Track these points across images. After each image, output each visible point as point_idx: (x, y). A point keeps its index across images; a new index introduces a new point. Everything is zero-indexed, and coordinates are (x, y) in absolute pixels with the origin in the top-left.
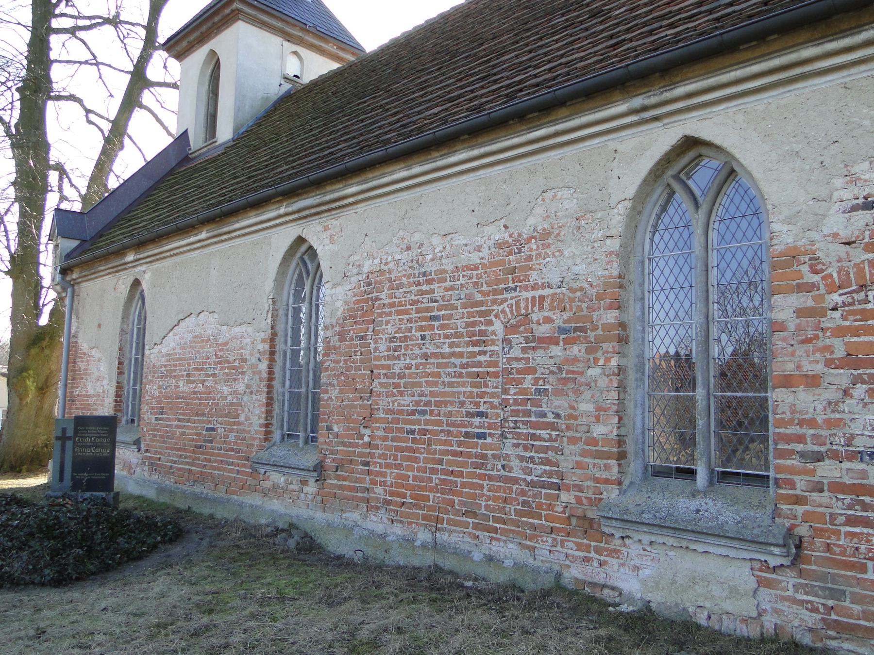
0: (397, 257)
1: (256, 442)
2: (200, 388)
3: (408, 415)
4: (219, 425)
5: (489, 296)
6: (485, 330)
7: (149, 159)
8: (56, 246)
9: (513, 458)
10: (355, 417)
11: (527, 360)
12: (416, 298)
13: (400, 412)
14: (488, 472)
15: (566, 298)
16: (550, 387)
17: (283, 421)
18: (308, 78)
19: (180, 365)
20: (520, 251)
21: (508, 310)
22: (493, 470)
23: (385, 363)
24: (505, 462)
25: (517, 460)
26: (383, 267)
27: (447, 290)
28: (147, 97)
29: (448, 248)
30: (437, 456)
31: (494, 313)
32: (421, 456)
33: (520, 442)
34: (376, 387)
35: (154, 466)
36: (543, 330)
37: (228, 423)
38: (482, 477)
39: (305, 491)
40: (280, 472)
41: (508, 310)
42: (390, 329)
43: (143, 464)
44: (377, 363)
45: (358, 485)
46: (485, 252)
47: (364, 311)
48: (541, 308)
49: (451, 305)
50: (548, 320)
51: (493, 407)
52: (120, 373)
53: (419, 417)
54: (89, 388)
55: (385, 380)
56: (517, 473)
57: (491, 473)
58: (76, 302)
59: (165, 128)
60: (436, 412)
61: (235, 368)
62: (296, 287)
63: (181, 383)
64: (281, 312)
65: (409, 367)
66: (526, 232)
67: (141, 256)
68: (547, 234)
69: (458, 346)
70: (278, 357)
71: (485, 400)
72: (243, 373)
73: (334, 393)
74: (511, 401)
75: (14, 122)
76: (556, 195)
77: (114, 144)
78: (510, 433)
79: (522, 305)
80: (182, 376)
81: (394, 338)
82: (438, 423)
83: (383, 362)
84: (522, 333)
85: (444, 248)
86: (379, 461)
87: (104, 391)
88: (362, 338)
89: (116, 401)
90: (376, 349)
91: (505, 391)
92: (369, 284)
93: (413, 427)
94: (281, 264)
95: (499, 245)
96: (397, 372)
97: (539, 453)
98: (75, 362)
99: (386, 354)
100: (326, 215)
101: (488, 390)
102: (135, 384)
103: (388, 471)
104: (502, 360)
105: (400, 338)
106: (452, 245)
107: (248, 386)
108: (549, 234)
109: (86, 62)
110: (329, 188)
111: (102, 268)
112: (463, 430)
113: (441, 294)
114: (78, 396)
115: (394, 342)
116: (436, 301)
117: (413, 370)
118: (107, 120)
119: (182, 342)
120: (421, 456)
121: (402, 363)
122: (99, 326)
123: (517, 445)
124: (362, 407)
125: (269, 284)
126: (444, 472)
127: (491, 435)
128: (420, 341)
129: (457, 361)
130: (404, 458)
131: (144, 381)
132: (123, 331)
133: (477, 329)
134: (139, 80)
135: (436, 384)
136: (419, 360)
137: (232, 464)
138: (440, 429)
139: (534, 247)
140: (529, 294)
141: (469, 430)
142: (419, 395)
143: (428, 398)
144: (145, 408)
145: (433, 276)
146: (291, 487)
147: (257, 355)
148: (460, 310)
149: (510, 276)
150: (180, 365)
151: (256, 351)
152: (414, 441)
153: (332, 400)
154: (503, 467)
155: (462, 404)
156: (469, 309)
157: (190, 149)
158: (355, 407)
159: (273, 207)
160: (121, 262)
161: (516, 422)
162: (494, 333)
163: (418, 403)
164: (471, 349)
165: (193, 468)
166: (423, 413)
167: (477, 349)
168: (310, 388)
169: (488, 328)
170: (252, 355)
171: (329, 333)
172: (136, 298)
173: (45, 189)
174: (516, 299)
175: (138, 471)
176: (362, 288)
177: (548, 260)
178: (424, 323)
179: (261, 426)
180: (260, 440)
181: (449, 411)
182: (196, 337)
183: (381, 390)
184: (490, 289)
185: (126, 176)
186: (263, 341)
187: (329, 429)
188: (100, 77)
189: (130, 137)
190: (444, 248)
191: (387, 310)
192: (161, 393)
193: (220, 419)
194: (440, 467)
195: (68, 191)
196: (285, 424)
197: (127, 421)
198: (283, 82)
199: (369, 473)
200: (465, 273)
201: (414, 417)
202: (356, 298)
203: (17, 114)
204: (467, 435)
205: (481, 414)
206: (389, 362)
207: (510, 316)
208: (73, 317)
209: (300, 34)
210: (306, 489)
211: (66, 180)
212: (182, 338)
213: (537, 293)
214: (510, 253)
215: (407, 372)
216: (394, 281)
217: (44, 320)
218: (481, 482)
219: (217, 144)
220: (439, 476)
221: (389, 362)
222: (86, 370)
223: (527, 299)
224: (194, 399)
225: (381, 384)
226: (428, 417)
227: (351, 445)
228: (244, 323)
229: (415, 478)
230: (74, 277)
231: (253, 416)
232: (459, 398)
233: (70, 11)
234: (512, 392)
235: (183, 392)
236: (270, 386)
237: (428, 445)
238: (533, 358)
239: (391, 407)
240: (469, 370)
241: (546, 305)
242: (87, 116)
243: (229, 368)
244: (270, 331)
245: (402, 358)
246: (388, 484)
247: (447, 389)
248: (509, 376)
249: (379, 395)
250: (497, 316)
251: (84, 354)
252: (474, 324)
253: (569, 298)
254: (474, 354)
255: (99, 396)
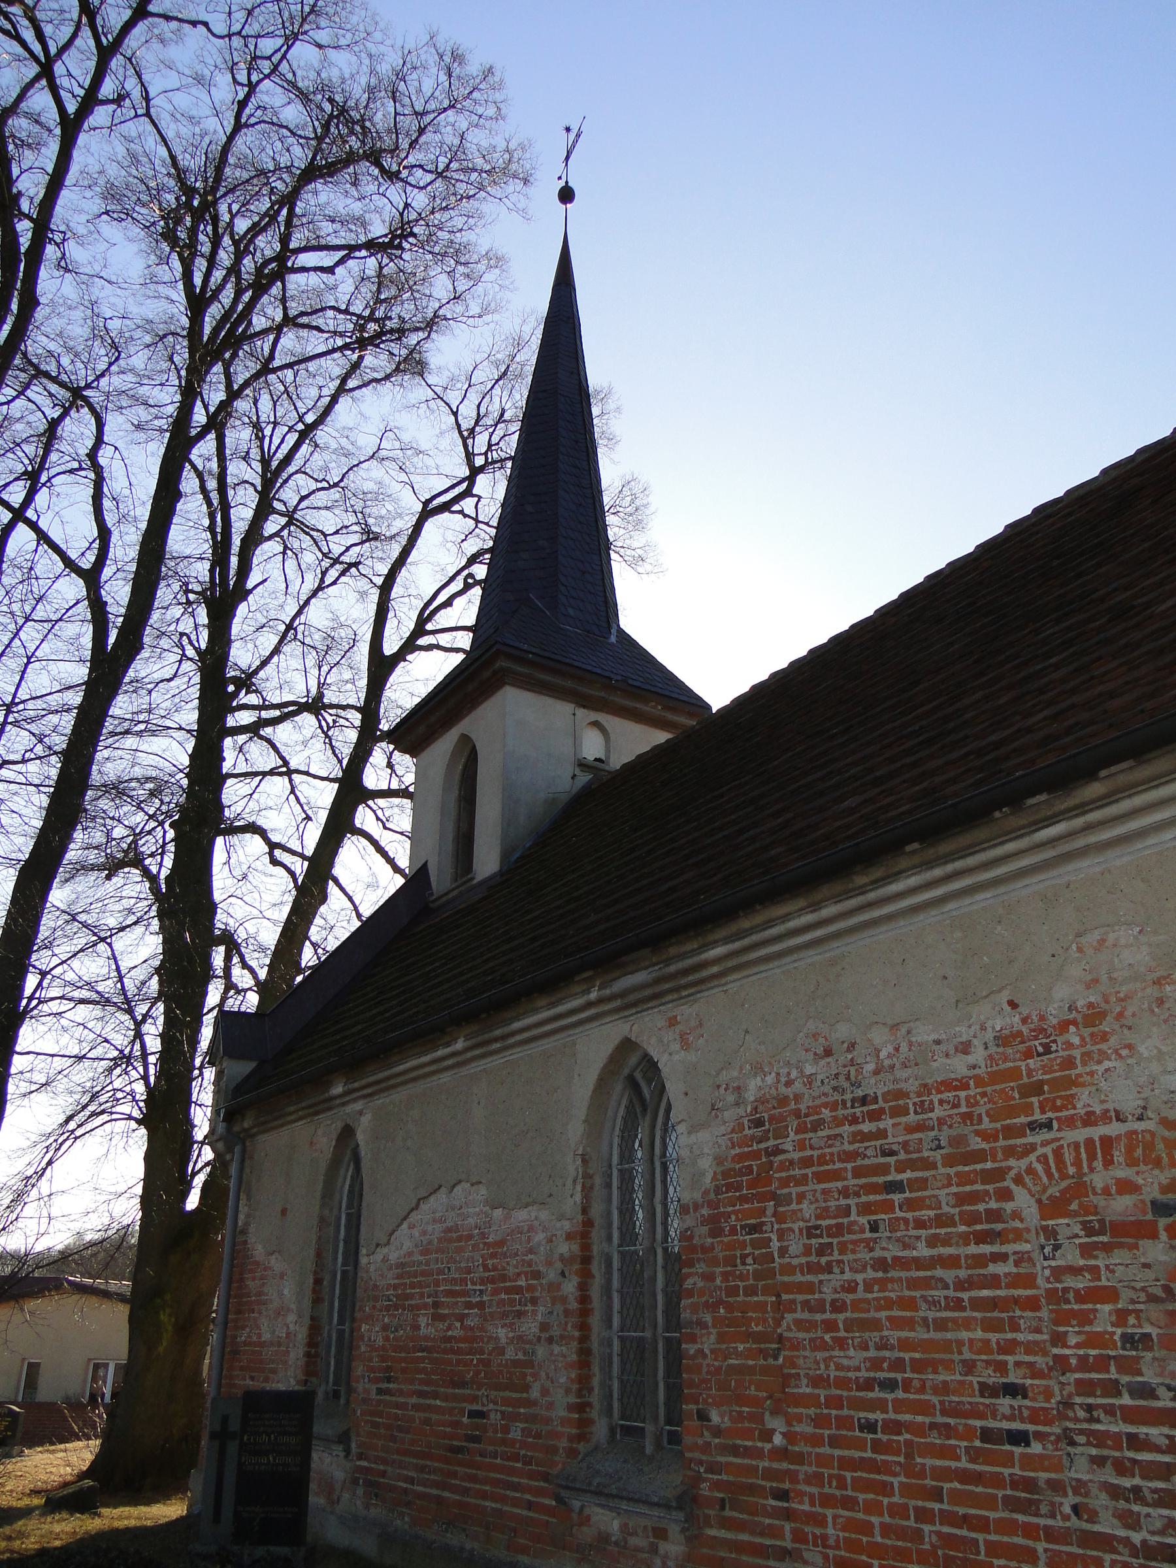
0: (809, 1069)
1: (563, 1443)
2: (457, 1331)
3: (859, 1389)
4: (491, 1406)
5: (996, 1139)
6: (998, 1210)
7: (367, 911)
8: (219, 1075)
9: (1094, 1491)
10: (753, 1391)
11: (1094, 1270)
12: (851, 1148)
13: (842, 1383)
14: (1042, 1522)
15: (1158, 1140)
16: (1154, 1332)
17: (611, 1396)
18: (618, 761)
19: (420, 1285)
20: (1047, 1050)
21: (1039, 1168)
22: (1053, 1516)
23: (802, 1279)
24: (1078, 1499)
25: (1104, 1496)
26: (783, 1090)
27: (910, 1129)
28: (364, 817)
29: (904, 1047)
30: (928, 1482)
31: (1012, 1173)
32: (895, 1481)
33: (1105, 1452)
34: (789, 1329)
35: (374, 1488)
36: (1121, 1206)
37: (507, 1402)
38: (1030, 1531)
39: (661, 1551)
40: (611, 1509)
41: (1039, 1168)
42: (807, 1209)
43: (355, 1482)
44: (786, 1279)
45: (768, 1542)
46: (978, 1055)
47: (752, 1176)
48: (1108, 1163)
49: (922, 1159)
50: (1126, 1187)
51: (1036, 1374)
52: (317, 1300)
53: (882, 1395)
54: (264, 1328)
55: (806, 1315)
56: (1106, 1525)
57: (1050, 1522)
58: (247, 1170)
59: (391, 861)
60: (916, 1384)
61: (518, 1290)
62: (622, 1131)
63: (423, 1321)
64: (598, 1180)
65: (851, 1287)
66: (1055, 1013)
67: (356, 1085)
68: (1094, 1016)
69: (946, 1242)
70: (596, 1268)
71: (1018, 1358)
72: (534, 1301)
73: (708, 1342)
74: (1073, 1361)
75: (164, 873)
76: (1104, 940)
77: (312, 896)
78: (1082, 1432)
79: (1068, 1157)
80: (425, 1306)
81: (817, 1227)
82: (924, 1408)
83: (799, 1278)
84: (1074, 1214)
85: (897, 1049)
86: (808, 1489)
87: (288, 1334)
88: (755, 1229)
89: (308, 1355)
90: (783, 1251)
91: (1059, 1339)
92: (759, 1123)
93: (872, 1416)
94: (594, 1091)
95: (1003, 1040)
96: (829, 1298)
97: (1151, 1479)
98: (242, 1280)
99: (803, 1260)
100: (670, 997)
101: (1020, 1337)
102: (341, 1321)
103: (829, 1513)
104: (1042, 1271)
105: (829, 1227)
106: (911, 1044)
107: (544, 1327)
108: (1103, 1015)
109: (272, 772)
110: (673, 951)
111: (292, 1109)
112: (978, 1423)
113: (900, 1139)
114: (245, 1343)
115: (817, 1236)
116: (892, 1153)
117: (861, 1293)
118: (302, 856)
119: (425, 1239)
120: (895, 1481)
121: (836, 1279)
122: (284, 1212)
123: (1099, 1461)
124: (765, 1370)
125: (575, 1130)
126: (948, 1518)
127: (1039, 1436)
128: (868, 1235)
129: (949, 1275)
130: (858, 1485)
131: (358, 1315)
132: (322, 1220)
133: (981, 1207)
134: (351, 792)
135: (909, 1324)
136: (871, 1274)
137: (516, 1487)
138: (927, 1420)
139: (1076, 1040)
140: (1080, 1134)
141: (991, 1424)
142: (879, 1348)
143: (897, 1354)
144: (359, 1369)
145: (881, 1103)
146: (634, 1541)
147: (559, 1265)
148: (942, 1170)
149: (1034, 1100)
150: (420, 1285)
151: (556, 1256)
152: (877, 1446)
153: (705, 1356)
154: (1075, 1509)
155: (969, 1367)
156: (960, 1168)
157: (432, 894)
158: (751, 1370)
159: (577, 989)
160: (322, 1097)
161: (1089, 1408)
162: (1016, 1215)
163: (876, 1364)
164: (973, 1249)
165: (446, 1494)
166: (890, 1385)
167: (986, 1249)
168: (660, 1330)
169: (1004, 1205)
170: (549, 1263)
171: (689, 1221)
172: (347, 1159)
173: (207, 975)
174: (1054, 1145)
175: (346, 1496)
176: (747, 1132)
177: (1107, 1064)
178: (872, 1198)
179: (570, 1408)
180: (571, 1439)
181: (945, 1383)
182: (449, 1230)
183: (801, 1335)
184: (998, 1125)
185: (332, 945)
186: (569, 1237)
187: (703, 1416)
188: (293, 792)
189: (336, 882)
190: (897, 1049)
191: (797, 1172)
192: (387, 1339)
193: (493, 1393)
194: (937, 1506)
195: (241, 977)
196: (616, 1404)
197: (327, 1393)
198: (578, 772)
199: (789, 1515)
200: (944, 1096)
201: (871, 1395)
202: (737, 1151)
203: (168, 862)
204: (987, 1435)
205: (1013, 1390)
206: (810, 1278)
207: (1045, 1179)
208: (242, 1196)
209: (602, 694)
210: (664, 1547)
211: (236, 960)
212: (424, 1233)
213: (1096, 1132)
214: (1028, 1054)
215: (849, 1298)
216: (807, 1115)
217: (193, 1202)
218: (1030, 1543)
219: (475, 882)
220: (937, 1528)
221: (810, 1278)
222: (260, 1294)
223: (1077, 1145)
224: (445, 1352)
225: (799, 1323)
226: (900, 1394)
227: (748, 1452)
228: (534, 1203)
229: (886, 1530)
230: (246, 1125)
231: (554, 1389)
232: (960, 1353)
233: (253, 699)
234: (1073, 1341)
235: (426, 1338)
236: (584, 1327)
237: (907, 1456)
238: (1107, 1267)
239: (822, 1371)
240: (974, 1293)
241: (1118, 1156)
242: (271, 854)
243: (508, 1291)
244: (580, 1218)
245: (836, 1270)
246: (831, 1542)
247: (932, 1335)
248: (1070, 1308)
249: (796, 1346)
250: (1018, 1180)
251: (257, 1263)
252: (974, 1198)
253: (1164, 1139)
254: (980, 1261)
255: (279, 1344)
